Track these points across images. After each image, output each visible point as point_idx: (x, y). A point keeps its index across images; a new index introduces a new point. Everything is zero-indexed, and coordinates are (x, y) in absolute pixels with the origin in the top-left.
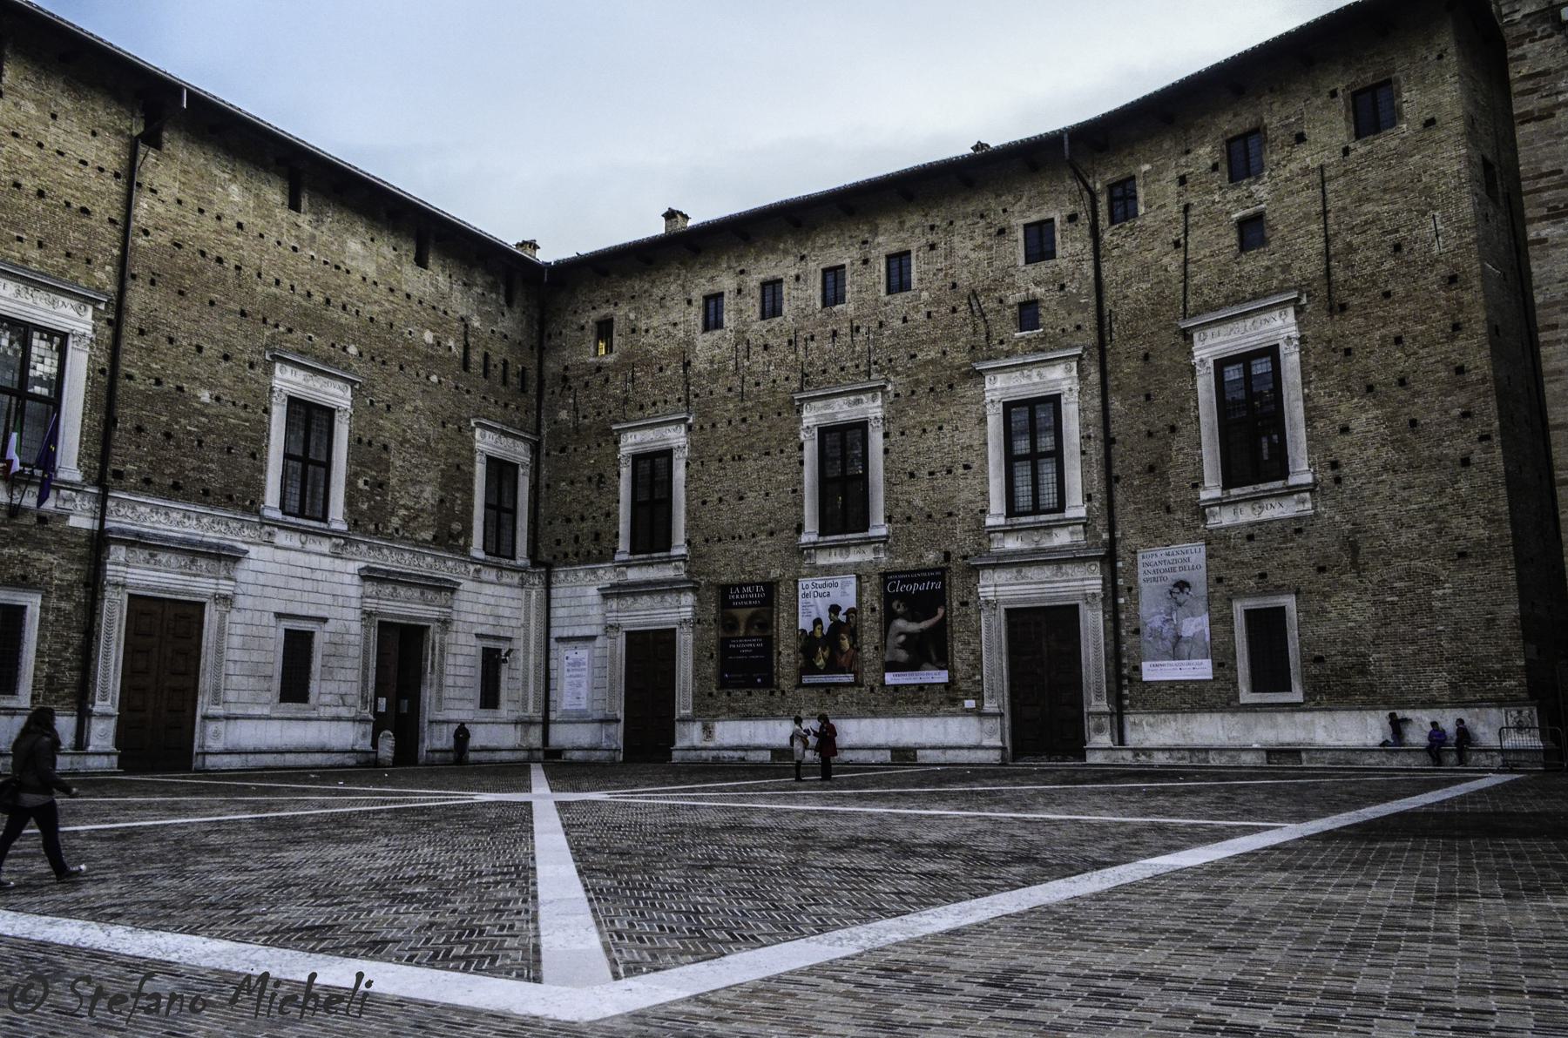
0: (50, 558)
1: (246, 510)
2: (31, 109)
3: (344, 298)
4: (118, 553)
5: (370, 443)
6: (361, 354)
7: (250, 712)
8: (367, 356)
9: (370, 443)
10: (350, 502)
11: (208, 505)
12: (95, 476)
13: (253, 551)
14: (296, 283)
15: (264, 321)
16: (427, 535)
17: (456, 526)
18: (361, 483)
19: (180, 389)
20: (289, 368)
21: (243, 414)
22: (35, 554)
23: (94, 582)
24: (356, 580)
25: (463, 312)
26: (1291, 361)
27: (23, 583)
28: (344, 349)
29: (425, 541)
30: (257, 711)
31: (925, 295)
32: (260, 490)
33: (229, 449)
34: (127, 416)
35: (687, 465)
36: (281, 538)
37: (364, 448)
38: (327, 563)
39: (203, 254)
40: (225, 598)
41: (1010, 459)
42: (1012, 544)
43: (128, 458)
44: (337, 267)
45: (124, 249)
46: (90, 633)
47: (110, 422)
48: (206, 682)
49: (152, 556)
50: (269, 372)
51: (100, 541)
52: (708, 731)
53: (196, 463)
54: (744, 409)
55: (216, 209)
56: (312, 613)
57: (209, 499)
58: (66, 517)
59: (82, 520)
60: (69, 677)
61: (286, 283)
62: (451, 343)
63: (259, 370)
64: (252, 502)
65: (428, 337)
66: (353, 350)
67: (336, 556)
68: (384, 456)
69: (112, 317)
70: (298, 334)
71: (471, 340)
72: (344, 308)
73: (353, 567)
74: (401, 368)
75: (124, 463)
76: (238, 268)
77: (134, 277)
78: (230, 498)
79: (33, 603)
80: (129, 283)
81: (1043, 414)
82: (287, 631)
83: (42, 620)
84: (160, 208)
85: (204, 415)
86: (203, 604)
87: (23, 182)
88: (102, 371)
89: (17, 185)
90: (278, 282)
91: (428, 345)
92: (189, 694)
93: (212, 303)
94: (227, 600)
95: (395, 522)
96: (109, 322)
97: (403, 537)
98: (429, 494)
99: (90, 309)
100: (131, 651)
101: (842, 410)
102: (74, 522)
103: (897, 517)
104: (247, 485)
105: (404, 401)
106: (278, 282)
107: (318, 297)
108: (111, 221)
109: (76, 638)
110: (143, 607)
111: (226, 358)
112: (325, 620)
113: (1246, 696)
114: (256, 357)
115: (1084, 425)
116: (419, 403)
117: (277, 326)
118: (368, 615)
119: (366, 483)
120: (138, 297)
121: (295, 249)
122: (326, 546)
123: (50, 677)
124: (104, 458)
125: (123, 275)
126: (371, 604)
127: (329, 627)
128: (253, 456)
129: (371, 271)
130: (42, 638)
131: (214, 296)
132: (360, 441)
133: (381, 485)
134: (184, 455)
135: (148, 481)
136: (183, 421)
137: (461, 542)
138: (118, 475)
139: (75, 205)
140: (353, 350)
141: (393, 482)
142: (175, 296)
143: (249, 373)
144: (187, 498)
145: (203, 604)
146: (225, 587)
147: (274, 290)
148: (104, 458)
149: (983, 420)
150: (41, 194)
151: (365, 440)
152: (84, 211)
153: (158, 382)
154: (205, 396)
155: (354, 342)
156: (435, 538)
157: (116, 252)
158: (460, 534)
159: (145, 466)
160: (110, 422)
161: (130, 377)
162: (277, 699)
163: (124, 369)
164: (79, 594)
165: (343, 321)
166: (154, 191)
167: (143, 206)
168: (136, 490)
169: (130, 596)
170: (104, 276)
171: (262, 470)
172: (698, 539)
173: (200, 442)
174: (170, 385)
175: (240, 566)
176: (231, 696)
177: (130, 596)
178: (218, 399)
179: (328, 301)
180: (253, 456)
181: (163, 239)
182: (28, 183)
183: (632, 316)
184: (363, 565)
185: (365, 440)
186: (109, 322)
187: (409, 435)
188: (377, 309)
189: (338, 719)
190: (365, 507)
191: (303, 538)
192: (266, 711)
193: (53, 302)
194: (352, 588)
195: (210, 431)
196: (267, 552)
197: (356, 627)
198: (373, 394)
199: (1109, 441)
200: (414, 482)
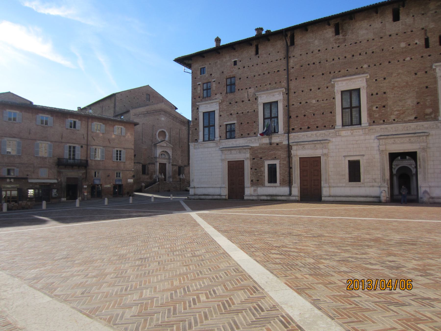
0: (280, 152)
1: (330, 129)
2: (265, 56)
3: (360, 51)
4: (294, 148)
5: (377, 94)
6: (369, 66)
7: (338, 185)
8: (372, 65)
9: (377, 94)
10: (370, 115)
11: (318, 130)
12: (287, 131)
13: (334, 140)
14: (340, 57)
15: (330, 73)
16: (412, 118)
17: (428, 111)
18: (374, 108)
19: (307, 102)
20: (340, 83)
21: (326, 102)
22: (276, 152)
23: (289, 156)
24: (376, 141)
25: (423, 26)
27: (275, 158)
28: (362, 67)
29: (411, 120)
30: (341, 185)
32: (335, 121)
33: (323, 113)
34: (293, 115)
36: (343, 133)
37: (375, 96)
38: (362, 138)
39: (309, 64)
40: (325, 154)
43: (294, 124)
44: (356, 43)
45: (288, 75)
46: (290, 168)
47: (290, 117)
48: (323, 178)
49: (303, 147)
50: (333, 86)
51: (289, 147)
53: (313, 120)
55: (311, 50)
56: (357, 154)
57: (318, 129)
58: (282, 142)
59: (285, 143)
60: (287, 179)
61: (336, 59)
62: (416, 41)
63: (329, 88)
64: (332, 126)
65: (403, 45)
66: (365, 66)
67: (365, 134)
68: (384, 95)
70: (343, 71)
71: (429, 35)
72: (360, 54)
73: (373, 137)
74: (389, 62)
75: (294, 126)
76: (320, 62)
77: (291, 80)
78: (325, 126)
79: (277, 162)
80: (290, 82)
82: (349, 161)
83: (280, 167)
84: (296, 60)
85: (314, 107)
86: (320, 157)
87: (265, 72)
88: (286, 106)
89: (264, 74)
90: (333, 60)
91: (403, 48)
92: (320, 181)
93: (313, 76)
94: (325, 155)
95: (393, 117)
96: (287, 94)
97: (397, 122)
98: (410, 102)
100: (302, 171)
102: (284, 143)
104: (330, 121)
105: (392, 74)
106: (333, 60)
107: (349, 56)
108: (285, 70)
109: (287, 169)
110: (303, 160)
111: (319, 89)
112: (363, 155)
114: (328, 85)
116: (400, 71)
117: (335, 72)
118: (381, 152)
119: (377, 107)
120: (292, 85)
121: (339, 47)
122: (361, 132)
123: (283, 179)
124: (289, 126)
125: (288, 80)
126: (382, 148)
127: (364, 158)
128: (331, 113)
129: (371, 36)
130: (280, 170)
131: (313, 74)
132: (372, 95)
133: (384, 107)
134: (310, 119)
135: (301, 129)
136: (308, 110)
137: (433, 116)
138: (293, 129)
139: (276, 71)
140: (365, 66)
141: (390, 103)
142: (303, 79)
143: (327, 90)
144: (312, 130)
145: (320, 157)
146: (325, 151)
147: (333, 62)
148: (289, 126)
150: (269, 73)
151: (374, 93)
152: (278, 71)
153: (300, 103)
154: (314, 101)
155: (366, 63)
156: (416, 118)
157: (286, 76)
158: (431, 114)
159: (299, 125)
161: (293, 105)
162: (348, 181)
163: (291, 103)
164: (287, 159)
165: (360, 59)
166: (294, 56)
167: (291, 61)
168: (298, 132)
169: (300, 158)
170: (284, 84)
171: (335, 116)
173: (314, 114)
174: (303, 103)
175: (330, 144)
176: (331, 181)
177: (300, 158)
178: (318, 101)
179: (353, 56)
180: (331, 113)
181: (298, 67)
182: (266, 72)
184: (376, 135)
185: (374, 93)
186: (287, 94)
187: (396, 84)
188: (375, 48)
189: (373, 186)
190: (377, 116)
191: (352, 132)
192: (344, 185)
193: (274, 96)
194: (375, 144)
195: (316, 110)
196: (339, 139)
197: (377, 156)
198: (376, 77)
200: (400, 101)
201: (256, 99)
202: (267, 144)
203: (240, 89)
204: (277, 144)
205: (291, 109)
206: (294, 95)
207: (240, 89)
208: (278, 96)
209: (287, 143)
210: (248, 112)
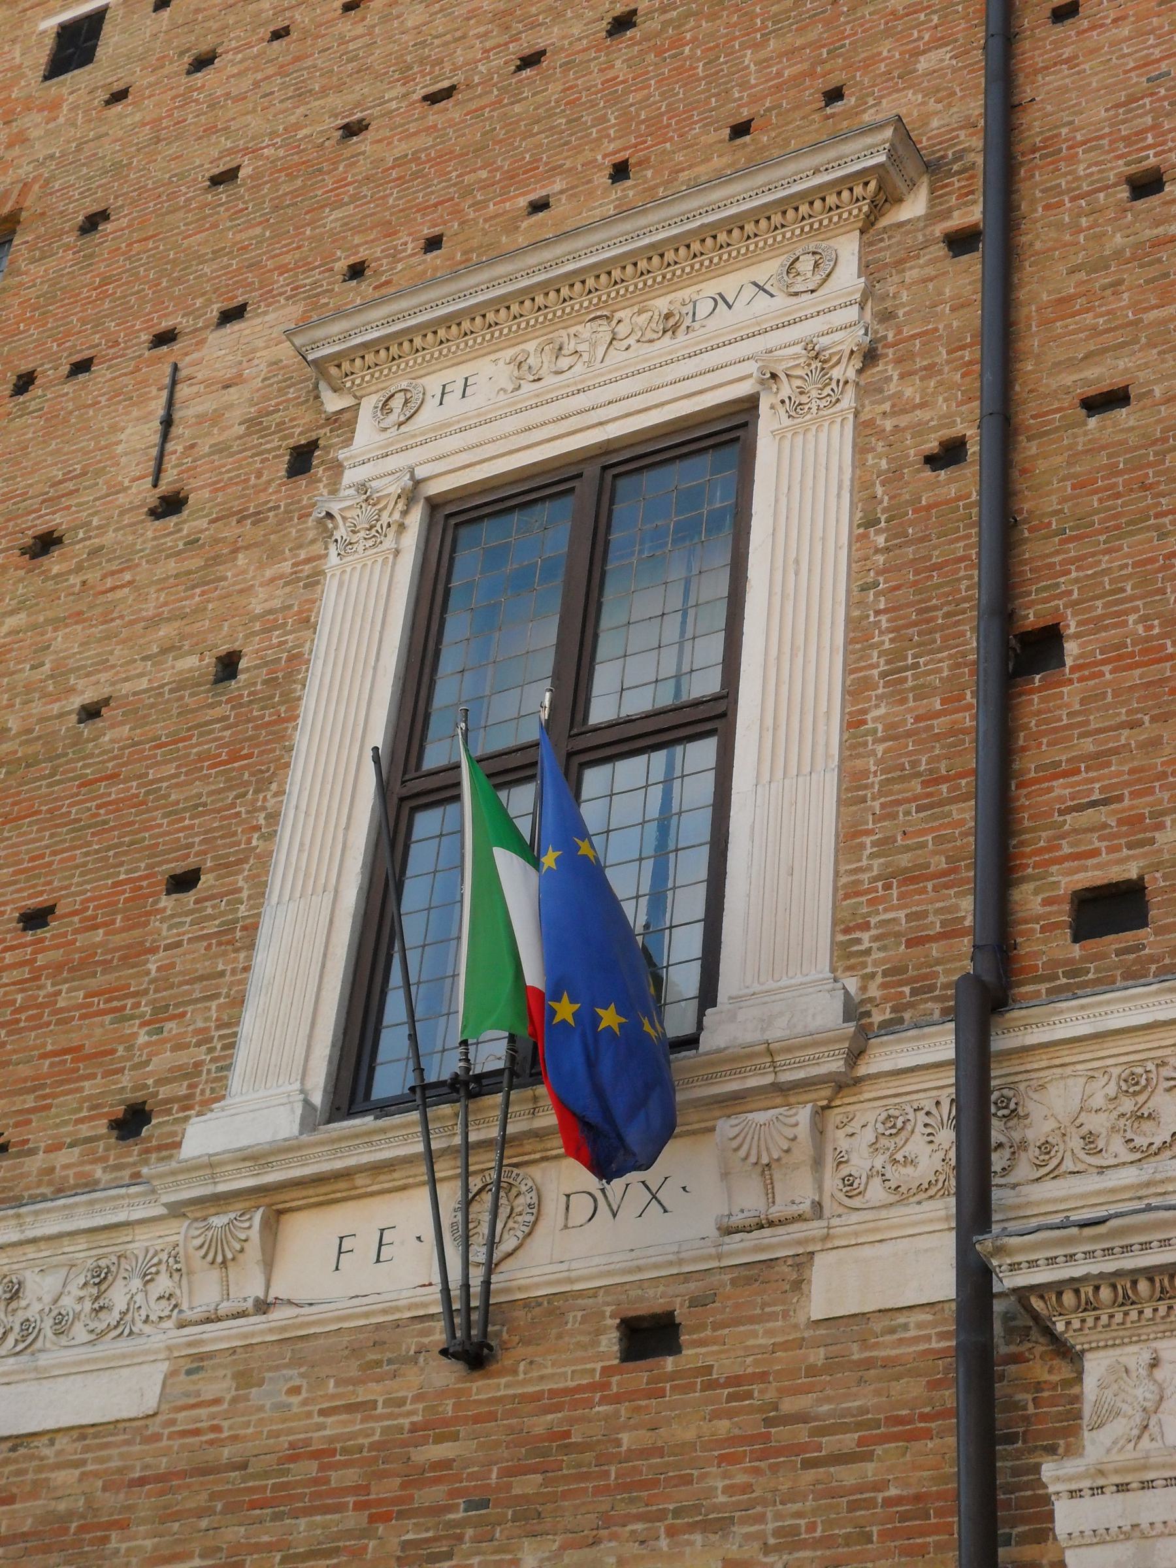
12: (956, 960)
47: (1026, 653)
69: (972, 214)
75: (1138, 829)
88: (949, 454)
99: (847, 249)
102: (838, 1287)
160: (1026, 653)
186: (961, 242)
201: (302, 460)
202: (373, 1346)
203: (51, 372)
204: (649, 1335)
205: (1047, 494)
206: (1127, 228)
207: (51, 372)
208: (774, 332)
209: (933, 1275)
210: (91, 713)
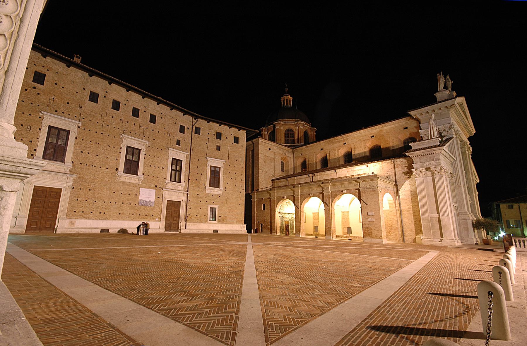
26: (222, 170)
31: (158, 127)
35: (76, 138)
41: (172, 170)
42: (170, 186)
52: (72, 223)
54: (103, 131)
81: (179, 163)
101: (135, 144)
103: (145, 173)
113: (209, 221)
115: (186, 168)
149: (167, 160)
172: (77, 162)
183: (56, 79)
199: (189, 172)
